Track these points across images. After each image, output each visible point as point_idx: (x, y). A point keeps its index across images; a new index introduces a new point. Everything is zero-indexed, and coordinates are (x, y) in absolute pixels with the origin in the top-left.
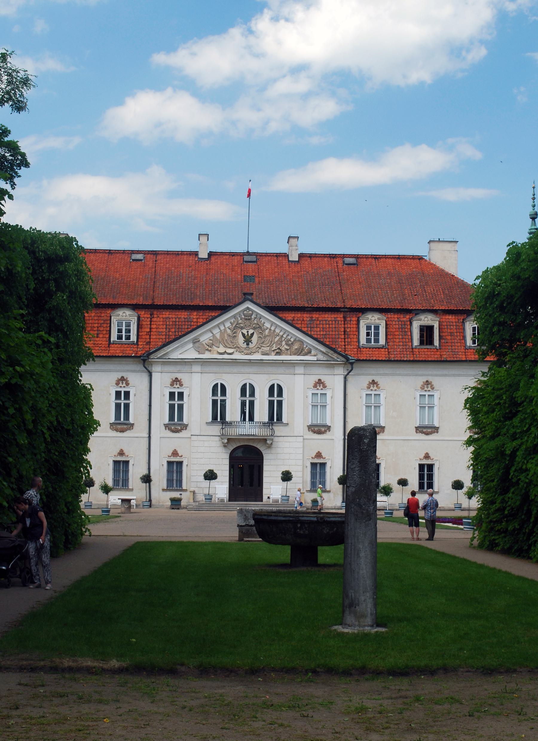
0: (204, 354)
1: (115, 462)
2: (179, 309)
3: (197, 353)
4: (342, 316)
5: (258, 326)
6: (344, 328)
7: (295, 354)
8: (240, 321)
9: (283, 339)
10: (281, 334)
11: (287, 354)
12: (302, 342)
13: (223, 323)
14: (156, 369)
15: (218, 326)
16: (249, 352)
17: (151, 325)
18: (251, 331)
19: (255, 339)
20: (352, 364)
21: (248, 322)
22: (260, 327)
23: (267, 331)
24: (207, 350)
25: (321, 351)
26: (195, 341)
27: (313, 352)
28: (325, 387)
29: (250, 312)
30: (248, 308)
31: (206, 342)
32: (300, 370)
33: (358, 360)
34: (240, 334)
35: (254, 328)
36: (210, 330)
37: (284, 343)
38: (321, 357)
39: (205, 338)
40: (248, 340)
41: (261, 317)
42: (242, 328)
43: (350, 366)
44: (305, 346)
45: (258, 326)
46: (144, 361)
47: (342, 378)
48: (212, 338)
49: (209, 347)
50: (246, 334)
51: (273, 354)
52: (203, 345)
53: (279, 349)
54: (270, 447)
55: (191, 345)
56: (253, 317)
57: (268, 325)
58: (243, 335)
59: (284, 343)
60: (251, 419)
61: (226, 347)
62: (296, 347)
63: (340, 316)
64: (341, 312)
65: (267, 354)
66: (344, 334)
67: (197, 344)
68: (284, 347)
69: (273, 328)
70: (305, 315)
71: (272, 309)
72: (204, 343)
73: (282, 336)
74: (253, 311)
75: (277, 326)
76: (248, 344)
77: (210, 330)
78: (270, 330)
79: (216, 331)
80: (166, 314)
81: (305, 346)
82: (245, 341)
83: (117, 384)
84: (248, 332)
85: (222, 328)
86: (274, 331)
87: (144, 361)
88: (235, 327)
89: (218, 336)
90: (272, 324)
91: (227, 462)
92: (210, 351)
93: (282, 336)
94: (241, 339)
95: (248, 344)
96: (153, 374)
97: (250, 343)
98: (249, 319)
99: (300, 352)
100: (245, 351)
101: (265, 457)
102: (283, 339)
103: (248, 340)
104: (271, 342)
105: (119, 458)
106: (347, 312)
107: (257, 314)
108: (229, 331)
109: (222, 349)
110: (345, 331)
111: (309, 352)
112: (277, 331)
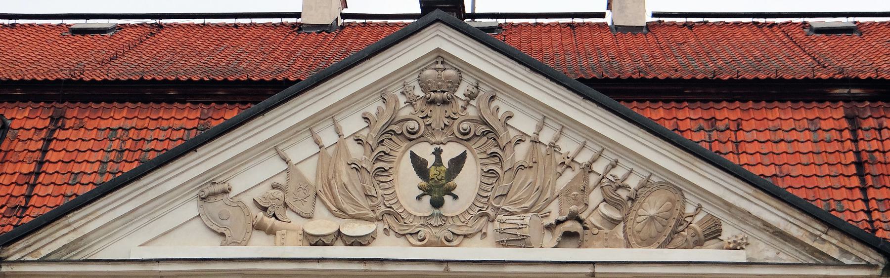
0: (246, 242)
2: (170, 101)
3: (219, 239)
4: (839, 113)
5: (482, 128)
6: (858, 153)
7: (647, 242)
8: (406, 112)
9: (593, 179)
10: (584, 158)
11: (608, 243)
12: (676, 188)
13: (331, 115)
15: (309, 127)
16: (442, 233)
17: (44, 151)
18: (451, 151)
19: (468, 181)
21: (438, 114)
22: (490, 132)
23: (521, 152)
24: (258, 227)
25: (766, 226)
26: (211, 193)
27: (728, 233)
29: (450, 72)
30: (440, 57)
31: (257, 194)
34: (406, 164)
35: (465, 137)
36: (275, 147)
37: (595, 197)
38: (764, 249)
39: (253, 181)
40: (437, 188)
41: (499, 88)
42: (412, 137)
44: (690, 209)
45: (482, 128)
48: (281, 180)
49: (267, 217)
50: (431, 160)
51: (549, 239)
52: (241, 206)
53: (574, 217)
55: (192, 209)
56: (460, 93)
58: (419, 166)
59: (595, 197)
61: (341, 213)
62: (652, 206)
63: (833, 116)
64: (835, 100)
65: (522, 241)
66: (861, 174)
67: (217, 206)
68: (596, 208)
69: (546, 137)
70: (681, 115)
72: (247, 200)
73: (588, 169)
74: (462, 68)
75: (566, 124)
76: (437, 204)
77: (275, 147)
78: (535, 142)
79: (301, 151)
80: (119, 117)
81: (690, 209)
82: (427, 191)
84: (438, 153)
85: (328, 137)
86: (553, 146)
88: (387, 131)
89: (309, 171)
90: (546, 114)
92: (271, 232)
93: (588, 169)
94: (407, 182)
95: (437, 204)
97: (447, 199)
98: (445, 102)
99: (673, 232)
100: (424, 232)
102: (593, 179)
103: (437, 188)
104: (541, 191)
106: (861, 100)
107: (481, 77)
108: (356, 152)
109: (324, 224)
110: (859, 164)
111: (713, 233)
112: (568, 146)
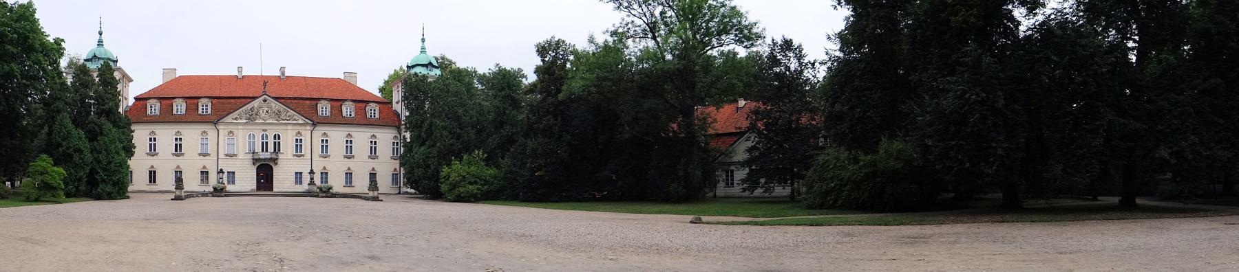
14: (220, 127)
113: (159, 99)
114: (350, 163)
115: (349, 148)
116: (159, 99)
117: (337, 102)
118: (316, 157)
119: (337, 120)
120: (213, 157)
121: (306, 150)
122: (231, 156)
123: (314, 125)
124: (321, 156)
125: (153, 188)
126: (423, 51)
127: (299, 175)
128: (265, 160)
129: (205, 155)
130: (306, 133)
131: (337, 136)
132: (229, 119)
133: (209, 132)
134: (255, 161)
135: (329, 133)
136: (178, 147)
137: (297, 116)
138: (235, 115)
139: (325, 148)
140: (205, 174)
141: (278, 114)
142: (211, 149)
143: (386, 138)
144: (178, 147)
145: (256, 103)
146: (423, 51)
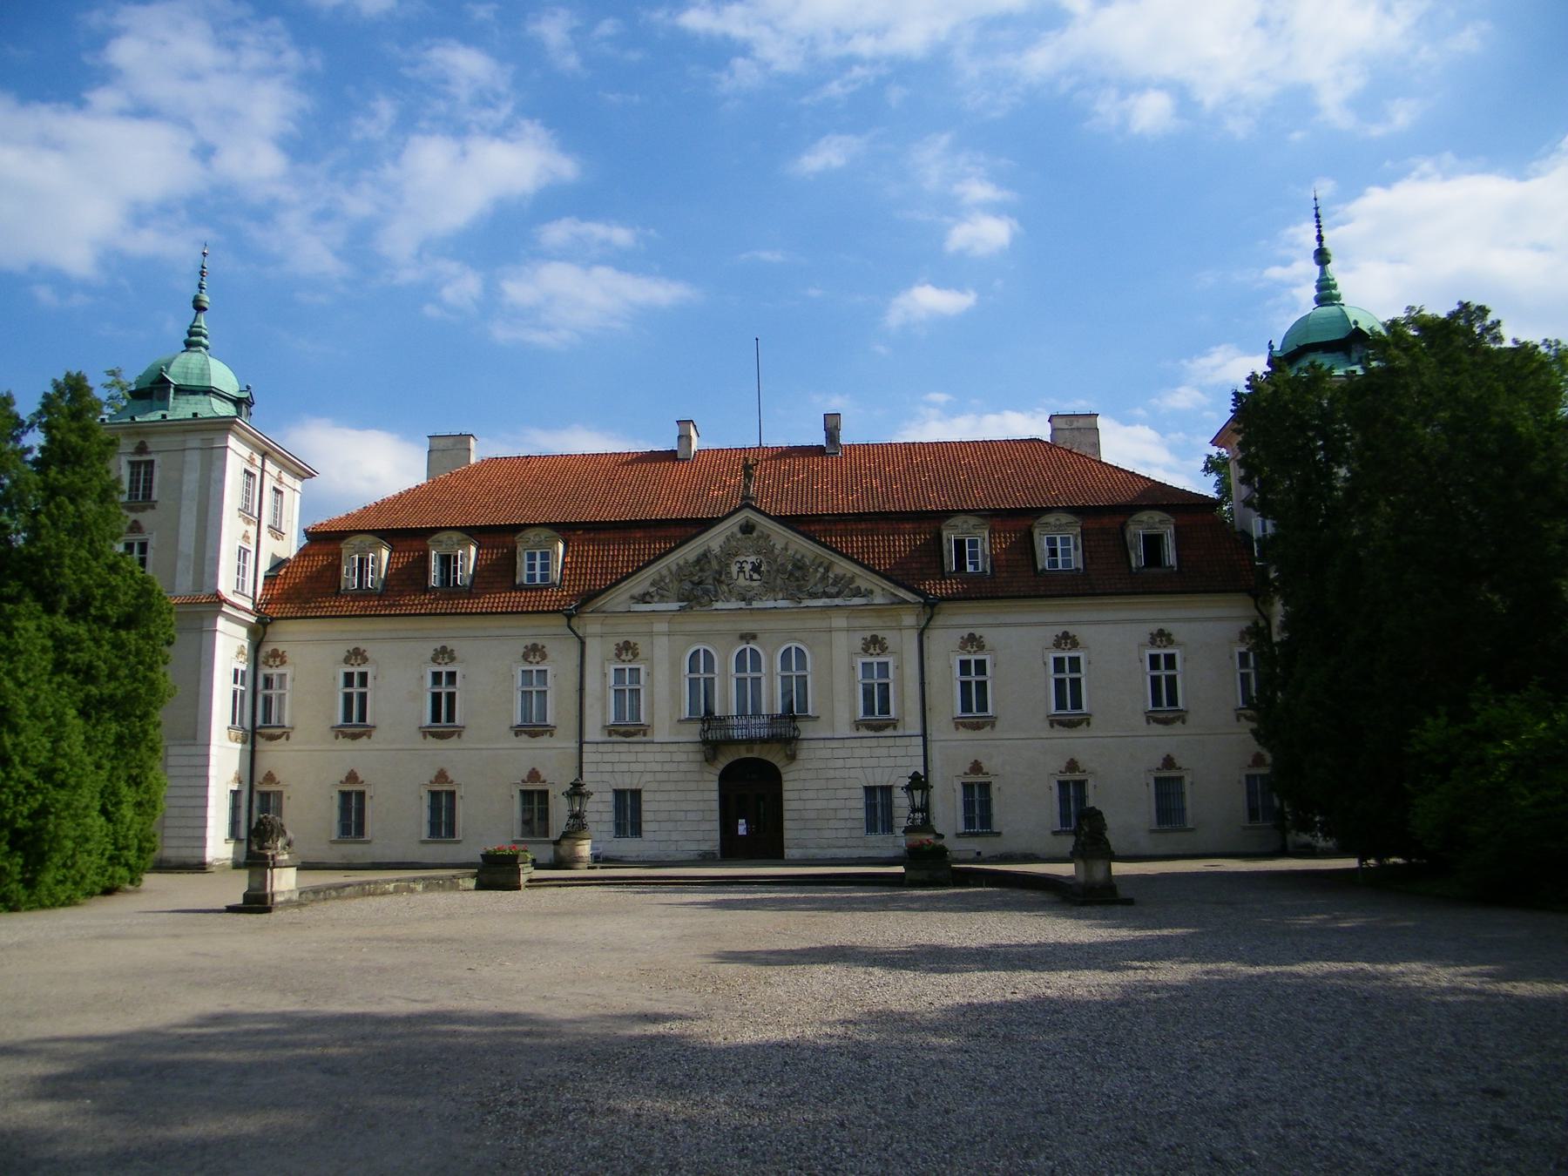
1: (523, 793)
14: (590, 626)
20: (933, 606)
28: (884, 649)
32: (839, 622)
33: (943, 599)
43: (928, 610)
46: (569, 617)
47: (914, 635)
54: (792, 758)
57: (778, 546)
60: (757, 713)
71: (788, 521)
83: (525, 657)
87: (569, 617)
91: (715, 786)
96: (588, 641)
101: (784, 777)
105: (530, 787)
113: (390, 536)
114: (1075, 743)
115: (1068, 692)
116: (390, 536)
117: (1016, 521)
118: (941, 728)
119: (1017, 580)
120: (564, 743)
121: (905, 704)
122: (628, 730)
123: (931, 606)
124: (960, 724)
125: (354, 851)
126: (1326, 293)
127: (877, 799)
128: (751, 741)
129: (532, 728)
130: (903, 642)
131: (1019, 642)
132: (618, 599)
133: (551, 648)
134: (711, 748)
135: (989, 635)
136: (443, 708)
137: (865, 580)
138: (641, 582)
139: (974, 695)
140: (534, 801)
141: (793, 580)
142: (557, 710)
143: (1209, 639)
144: (443, 708)
145: (713, 540)
146: (1326, 293)
